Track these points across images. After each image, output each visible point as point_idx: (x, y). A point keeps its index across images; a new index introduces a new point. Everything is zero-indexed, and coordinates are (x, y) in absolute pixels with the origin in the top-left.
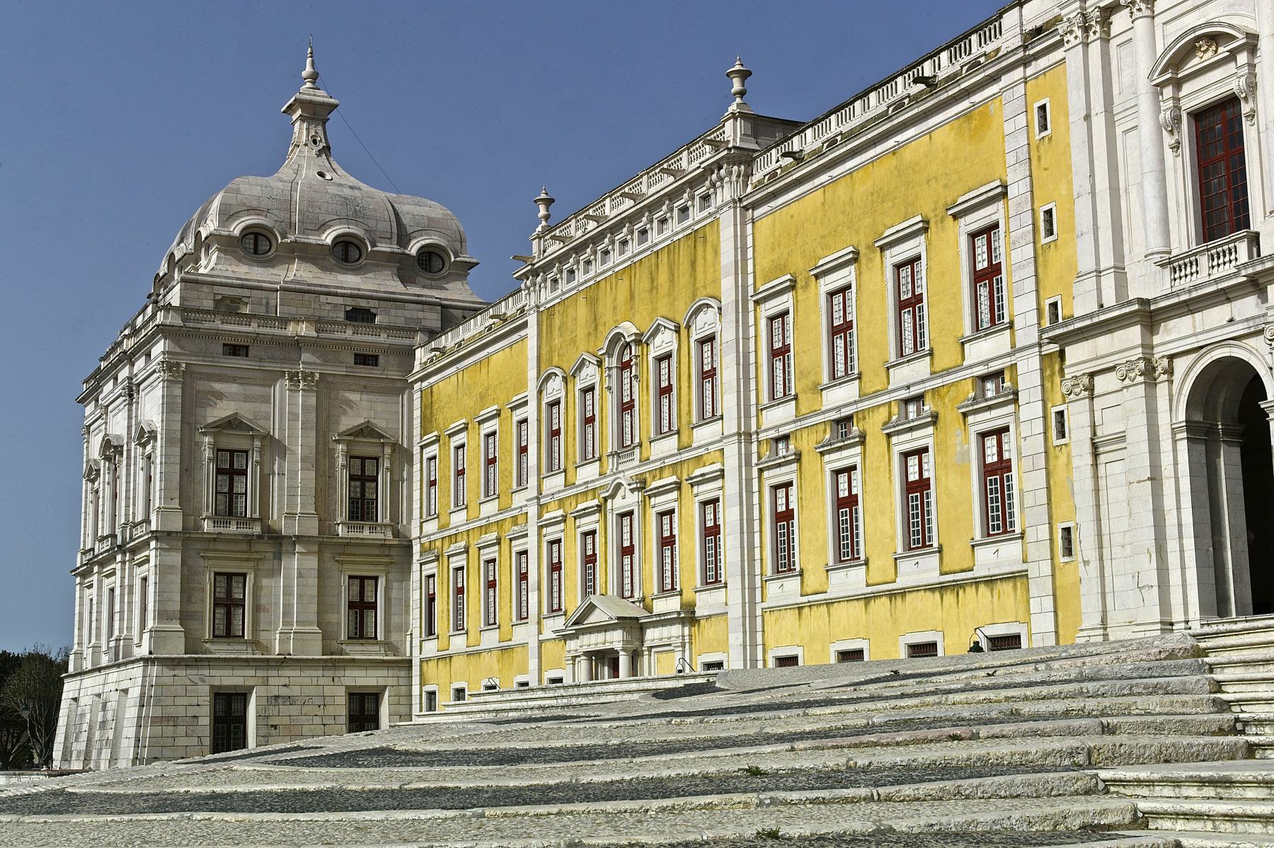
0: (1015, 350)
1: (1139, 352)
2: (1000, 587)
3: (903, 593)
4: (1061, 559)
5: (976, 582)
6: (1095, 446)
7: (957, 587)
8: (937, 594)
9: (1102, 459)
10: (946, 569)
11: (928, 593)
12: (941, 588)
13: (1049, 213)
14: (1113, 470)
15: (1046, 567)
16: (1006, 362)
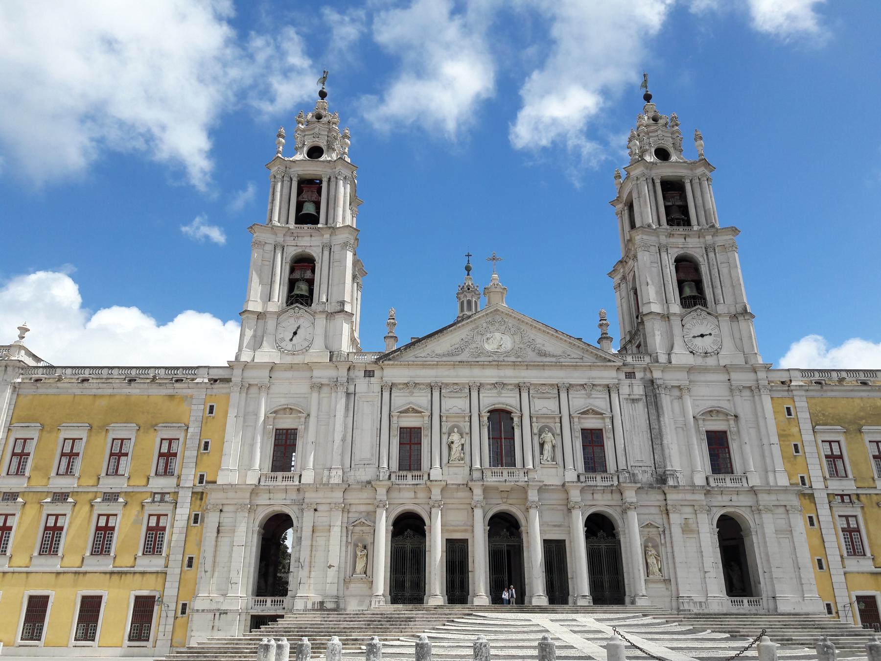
0: (178, 485)
1: (248, 501)
2: (148, 576)
3: (85, 573)
4: (185, 568)
5: (135, 573)
6: (218, 532)
7: (119, 573)
8: (108, 576)
9: (220, 535)
10: (116, 565)
11: (103, 575)
12: (112, 573)
13: (207, 444)
14: (224, 540)
15: (178, 571)
16: (173, 490)
